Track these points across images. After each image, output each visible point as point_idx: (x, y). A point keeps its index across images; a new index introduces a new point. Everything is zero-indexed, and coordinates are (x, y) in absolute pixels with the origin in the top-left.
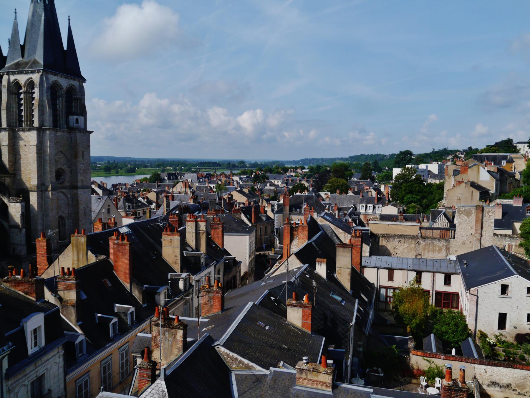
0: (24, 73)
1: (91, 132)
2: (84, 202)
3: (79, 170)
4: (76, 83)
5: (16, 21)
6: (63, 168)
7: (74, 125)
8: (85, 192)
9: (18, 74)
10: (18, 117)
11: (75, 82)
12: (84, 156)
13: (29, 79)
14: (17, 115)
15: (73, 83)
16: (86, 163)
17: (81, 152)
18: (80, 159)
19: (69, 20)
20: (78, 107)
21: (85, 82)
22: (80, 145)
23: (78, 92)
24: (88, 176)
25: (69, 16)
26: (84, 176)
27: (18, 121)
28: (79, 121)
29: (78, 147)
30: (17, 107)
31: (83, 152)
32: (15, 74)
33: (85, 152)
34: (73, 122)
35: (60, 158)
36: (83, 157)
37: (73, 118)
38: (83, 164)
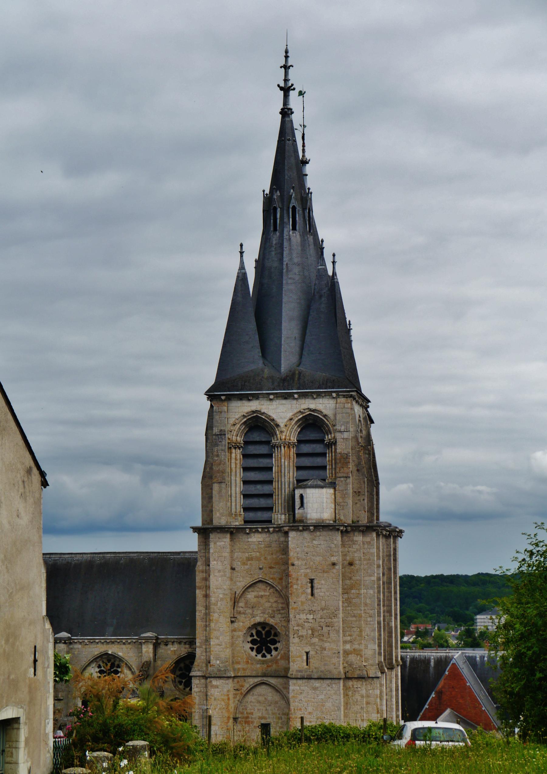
2: (310, 713)
3: (296, 628)
6: (272, 621)
8: (315, 689)
11: (320, 400)
12: (315, 591)
15: (312, 406)
16: (323, 609)
17: (305, 581)
22: (296, 563)
24: (327, 645)
26: (313, 644)
29: (291, 568)
31: (312, 581)
33: (315, 581)
35: (262, 596)
36: (312, 594)
38: (311, 612)
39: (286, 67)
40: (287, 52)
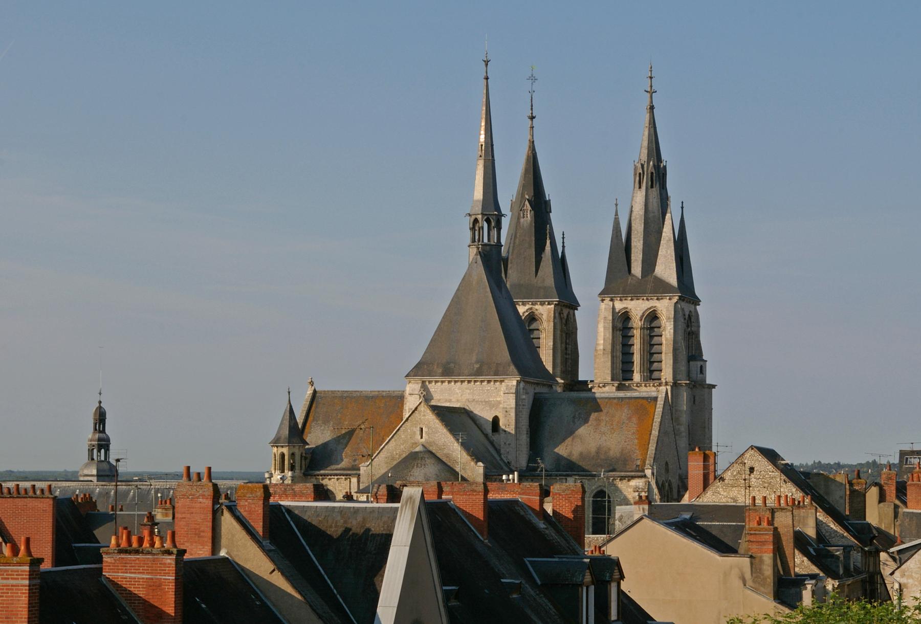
0: (643, 299)
1: (714, 386)
4: (692, 307)
5: (617, 217)
7: (698, 376)
9: (632, 300)
10: (621, 365)
13: (650, 308)
14: (621, 363)
18: (707, 430)
19: (682, 208)
20: (693, 345)
21: (699, 305)
23: (693, 322)
25: (682, 202)
27: (621, 371)
28: (704, 369)
30: (621, 350)
32: (626, 299)
34: (697, 372)
37: (697, 365)
39: (651, 78)
40: (651, 68)
